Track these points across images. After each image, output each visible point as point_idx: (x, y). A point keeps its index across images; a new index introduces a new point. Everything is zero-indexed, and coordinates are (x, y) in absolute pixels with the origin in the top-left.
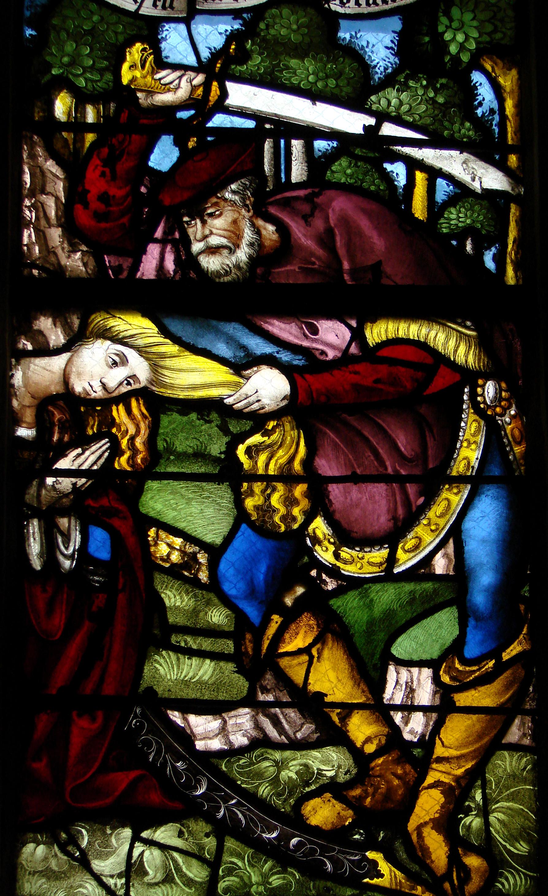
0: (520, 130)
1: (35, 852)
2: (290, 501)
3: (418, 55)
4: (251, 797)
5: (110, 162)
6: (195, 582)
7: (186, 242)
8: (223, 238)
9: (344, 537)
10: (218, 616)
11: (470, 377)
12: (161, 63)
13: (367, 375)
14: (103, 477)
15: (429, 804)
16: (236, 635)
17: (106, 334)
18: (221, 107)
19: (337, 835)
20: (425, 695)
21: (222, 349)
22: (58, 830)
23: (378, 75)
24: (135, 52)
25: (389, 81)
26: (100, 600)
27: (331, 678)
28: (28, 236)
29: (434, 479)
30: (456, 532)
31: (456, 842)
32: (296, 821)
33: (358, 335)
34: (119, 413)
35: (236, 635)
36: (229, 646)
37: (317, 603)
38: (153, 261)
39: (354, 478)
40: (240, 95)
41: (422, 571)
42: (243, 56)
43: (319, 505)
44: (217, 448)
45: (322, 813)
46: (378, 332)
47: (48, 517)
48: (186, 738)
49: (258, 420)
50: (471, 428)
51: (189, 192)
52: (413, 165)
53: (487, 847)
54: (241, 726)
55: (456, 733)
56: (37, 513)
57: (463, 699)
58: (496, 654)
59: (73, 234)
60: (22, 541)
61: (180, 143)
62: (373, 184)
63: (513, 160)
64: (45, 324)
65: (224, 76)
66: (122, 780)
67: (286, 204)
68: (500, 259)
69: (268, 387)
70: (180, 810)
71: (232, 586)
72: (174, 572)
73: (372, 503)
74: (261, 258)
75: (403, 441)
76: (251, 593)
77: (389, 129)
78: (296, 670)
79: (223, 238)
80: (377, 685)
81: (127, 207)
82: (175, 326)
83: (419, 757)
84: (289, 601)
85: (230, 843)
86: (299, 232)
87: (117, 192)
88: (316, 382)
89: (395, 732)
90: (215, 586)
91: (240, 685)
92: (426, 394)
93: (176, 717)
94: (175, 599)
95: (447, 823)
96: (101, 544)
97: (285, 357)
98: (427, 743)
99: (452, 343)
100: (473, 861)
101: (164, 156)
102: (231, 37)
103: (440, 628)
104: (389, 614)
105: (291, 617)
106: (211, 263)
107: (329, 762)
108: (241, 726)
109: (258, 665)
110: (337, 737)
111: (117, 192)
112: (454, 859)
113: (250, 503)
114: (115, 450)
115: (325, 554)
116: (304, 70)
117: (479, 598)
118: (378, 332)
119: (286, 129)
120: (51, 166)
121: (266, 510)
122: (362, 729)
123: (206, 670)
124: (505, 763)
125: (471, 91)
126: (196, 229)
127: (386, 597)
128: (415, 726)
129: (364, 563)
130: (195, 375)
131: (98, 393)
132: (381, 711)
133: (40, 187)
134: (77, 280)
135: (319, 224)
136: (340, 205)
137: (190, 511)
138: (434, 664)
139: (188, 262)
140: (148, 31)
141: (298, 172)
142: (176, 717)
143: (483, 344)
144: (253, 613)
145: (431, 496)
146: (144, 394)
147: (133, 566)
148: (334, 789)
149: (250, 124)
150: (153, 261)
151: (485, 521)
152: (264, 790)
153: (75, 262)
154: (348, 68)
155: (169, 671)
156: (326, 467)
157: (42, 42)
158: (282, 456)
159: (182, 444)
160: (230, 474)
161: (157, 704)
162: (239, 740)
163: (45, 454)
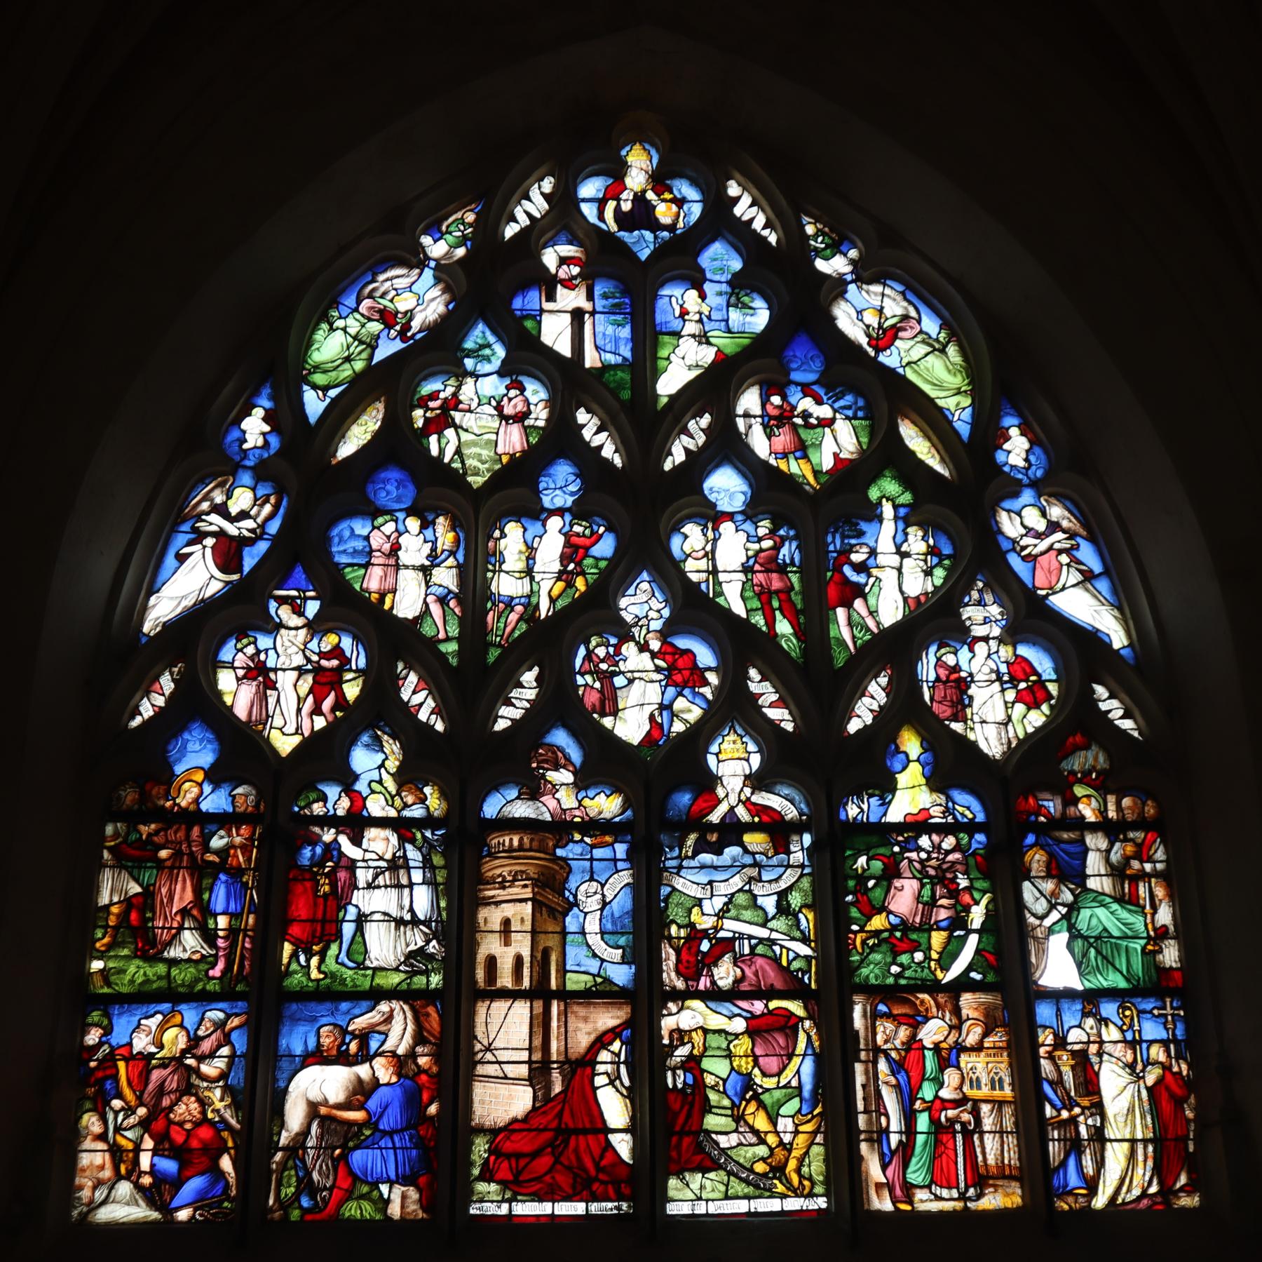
0: (815, 933)
1: (673, 1182)
2: (747, 1063)
3: (783, 908)
4: (737, 1163)
5: (689, 949)
6: (718, 1091)
7: (712, 975)
8: (725, 974)
9: (764, 1074)
10: (726, 1102)
11: (801, 1019)
12: (703, 914)
13: (770, 1019)
14: (691, 1057)
15: (792, 1164)
16: (732, 1109)
17: (688, 1008)
18: (722, 929)
19: (765, 1175)
20: (791, 1128)
21: (725, 1012)
22: (679, 1174)
23: (770, 916)
24: (696, 910)
25: (774, 918)
26: (690, 1098)
27: (761, 1123)
28: (665, 975)
29: (790, 1056)
30: (798, 1072)
31: (801, 1176)
32: (751, 1170)
33: (766, 1006)
34: (694, 1034)
35: (732, 1109)
36: (729, 1112)
37: (756, 1097)
38: (704, 983)
39: (767, 1055)
40: (728, 924)
41: (786, 1086)
42: (728, 911)
43: (756, 1063)
44: (724, 1045)
45: (760, 1168)
46: (773, 1004)
47: (674, 1070)
48: (717, 1143)
49: (737, 1036)
50: (802, 1038)
51: (712, 959)
52: (782, 947)
53: (810, 1179)
54: (734, 1139)
55: (801, 1139)
56: (670, 1069)
57: (801, 1128)
58: (811, 1113)
59: (678, 973)
60: (666, 1078)
61: (710, 941)
62: (770, 954)
63: (813, 944)
64: (670, 1005)
65: (722, 918)
66: (698, 1158)
67: (743, 961)
68: (810, 979)
69: (739, 1025)
70: (716, 1166)
71: (730, 1092)
72: (712, 1088)
73: (772, 1064)
74: (737, 981)
75: (782, 1041)
76: (736, 1094)
77: (775, 935)
78: (750, 1119)
79: (725, 974)
80: (775, 1125)
81: (695, 965)
82: (711, 1004)
83: (788, 1148)
84: (748, 1096)
85: (732, 1178)
86: (748, 972)
87: (692, 959)
88: (754, 1022)
89: (781, 1140)
90: (725, 1092)
91: (734, 1125)
92: (788, 1025)
93: (714, 1136)
94: (713, 1097)
95: (798, 1171)
96: (690, 1080)
97: (744, 1014)
98: (791, 1144)
99: (796, 1007)
100: (806, 1183)
101: (705, 946)
102: (726, 904)
103: (794, 1105)
104: (778, 1100)
105: (748, 1102)
106: (720, 983)
107: (762, 1151)
108: (734, 1139)
109: (739, 1118)
110: (762, 1141)
111: (692, 959)
112: (800, 1182)
113: (735, 1064)
114: (693, 1047)
115: (758, 1080)
116: (747, 914)
117: (806, 1094)
118: (773, 1004)
119: (741, 937)
120: (671, 951)
121: (740, 1066)
122: (772, 1139)
123: (723, 1120)
124: (816, 1150)
125: (798, 921)
126: (715, 971)
127: (778, 1094)
128: (787, 1138)
129: (770, 1083)
130: (716, 1022)
131: (687, 1028)
132: (777, 1133)
133: (668, 959)
134: (680, 991)
135: (753, 968)
136: (760, 962)
137: (716, 1067)
138: (793, 1117)
139: (713, 983)
140: (699, 902)
141: (747, 951)
142: (714, 1136)
143: (806, 1008)
144: (737, 1102)
145: (790, 1059)
146: (701, 1028)
147: (699, 1086)
148: (763, 1159)
149: (731, 935)
150: (704, 983)
151: (808, 1067)
152: (742, 1161)
153: (680, 984)
154: (760, 912)
155: (711, 1121)
156: (758, 1052)
157: (666, 907)
158: (744, 1047)
159: (714, 1045)
160: (729, 1056)
161: (708, 1132)
162: (734, 1144)
163: (672, 1047)
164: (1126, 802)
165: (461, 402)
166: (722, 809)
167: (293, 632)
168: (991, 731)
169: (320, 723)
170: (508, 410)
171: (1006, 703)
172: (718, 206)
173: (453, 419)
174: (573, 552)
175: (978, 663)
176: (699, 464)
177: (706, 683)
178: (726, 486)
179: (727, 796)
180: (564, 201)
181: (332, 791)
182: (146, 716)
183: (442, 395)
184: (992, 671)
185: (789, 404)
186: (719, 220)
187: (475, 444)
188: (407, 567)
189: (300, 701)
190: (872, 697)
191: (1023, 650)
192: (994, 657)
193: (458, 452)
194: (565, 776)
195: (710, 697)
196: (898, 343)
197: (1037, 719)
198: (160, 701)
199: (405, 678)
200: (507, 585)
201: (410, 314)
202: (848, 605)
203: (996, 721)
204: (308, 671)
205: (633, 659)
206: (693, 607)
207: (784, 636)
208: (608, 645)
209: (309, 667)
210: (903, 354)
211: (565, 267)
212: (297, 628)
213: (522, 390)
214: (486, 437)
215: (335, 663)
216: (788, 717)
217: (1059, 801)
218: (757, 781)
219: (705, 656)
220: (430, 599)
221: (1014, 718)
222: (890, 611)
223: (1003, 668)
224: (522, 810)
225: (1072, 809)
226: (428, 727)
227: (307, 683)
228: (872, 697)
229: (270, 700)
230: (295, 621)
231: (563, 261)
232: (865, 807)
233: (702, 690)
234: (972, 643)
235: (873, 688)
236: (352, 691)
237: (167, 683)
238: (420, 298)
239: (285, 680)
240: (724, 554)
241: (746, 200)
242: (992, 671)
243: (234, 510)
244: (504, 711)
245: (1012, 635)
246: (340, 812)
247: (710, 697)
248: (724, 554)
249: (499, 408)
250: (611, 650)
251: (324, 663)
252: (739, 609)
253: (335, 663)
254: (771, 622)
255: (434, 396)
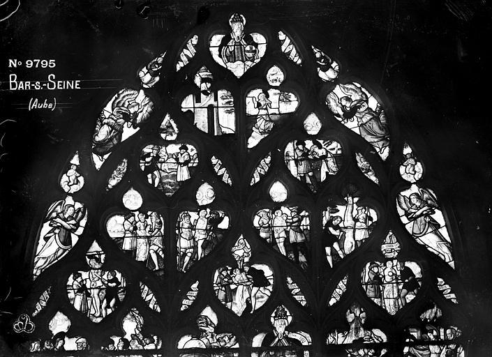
164: (448, 331)
165: (160, 157)
166: (277, 339)
167: (96, 271)
168: (392, 302)
169: (109, 311)
170: (181, 160)
171: (398, 290)
172: (274, 44)
173: (157, 166)
174: (214, 222)
175: (389, 271)
176: (267, 180)
177: (270, 284)
178: (278, 191)
179: (278, 335)
180: (203, 48)
181: (116, 339)
182: (39, 310)
183: (152, 155)
184: (393, 274)
185: (307, 149)
186: (275, 56)
187: (167, 177)
188: (140, 237)
189: (101, 302)
190: (340, 289)
191: (407, 264)
192: (395, 268)
193: (161, 179)
194: (210, 329)
195: (271, 290)
196: (357, 115)
197: (410, 297)
198: (44, 304)
199: (143, 289)
200: (184, 243)
201: (136, 114)
202: (331, 246)
203: (391, 299)
204: (104, 289)
205: (239, 276)
206: (264, 250)
207: (302, 262)
208: (227, 270)
209: (104, 287)
210: (359, 120)
211: (204, 84)
212: (98, 269)
213: (187, 149)
214: (172, 173)
215: (114, 284)
216: (304, 299)
217: (419, 332)
218: (290, 328)
219: (268, 272)
220: (151, 252)
221: (402, 295)
222: (349, 245)
223: (399, 273)
224: (194, 344)
225: (425, 335)
226: (154, 311)
227: (103, 294)
228: (340, 289)
229: (89, 302)
230: (98, 266)
231: (203, 80)
232: (336, 338)
233: (268, 288)
234: (385, 260)
235: (341, 284)
236: (121, 297)
237: (46, 295)
238: (139, 102)
239: (94, 292)
240: (280, 223)
241: (288, 41)
242: (393, 274)
243: (66, 216)
244: (185, 302)
245: (402, 257)
246: (120, 348)
247: (271, 290)
248: (280, 223)
249: (177, 159)
250: (229, 272)
251: (110, 284)
252: (283, 251)
253: (114, 284)
254: (297, 257)
255: (148, 155)
